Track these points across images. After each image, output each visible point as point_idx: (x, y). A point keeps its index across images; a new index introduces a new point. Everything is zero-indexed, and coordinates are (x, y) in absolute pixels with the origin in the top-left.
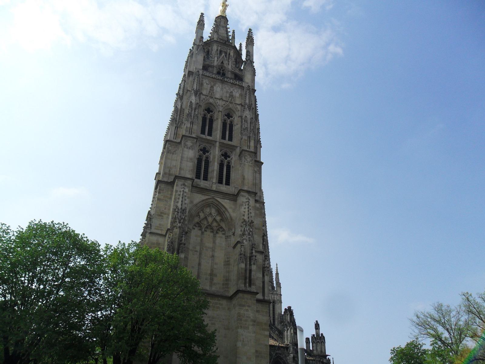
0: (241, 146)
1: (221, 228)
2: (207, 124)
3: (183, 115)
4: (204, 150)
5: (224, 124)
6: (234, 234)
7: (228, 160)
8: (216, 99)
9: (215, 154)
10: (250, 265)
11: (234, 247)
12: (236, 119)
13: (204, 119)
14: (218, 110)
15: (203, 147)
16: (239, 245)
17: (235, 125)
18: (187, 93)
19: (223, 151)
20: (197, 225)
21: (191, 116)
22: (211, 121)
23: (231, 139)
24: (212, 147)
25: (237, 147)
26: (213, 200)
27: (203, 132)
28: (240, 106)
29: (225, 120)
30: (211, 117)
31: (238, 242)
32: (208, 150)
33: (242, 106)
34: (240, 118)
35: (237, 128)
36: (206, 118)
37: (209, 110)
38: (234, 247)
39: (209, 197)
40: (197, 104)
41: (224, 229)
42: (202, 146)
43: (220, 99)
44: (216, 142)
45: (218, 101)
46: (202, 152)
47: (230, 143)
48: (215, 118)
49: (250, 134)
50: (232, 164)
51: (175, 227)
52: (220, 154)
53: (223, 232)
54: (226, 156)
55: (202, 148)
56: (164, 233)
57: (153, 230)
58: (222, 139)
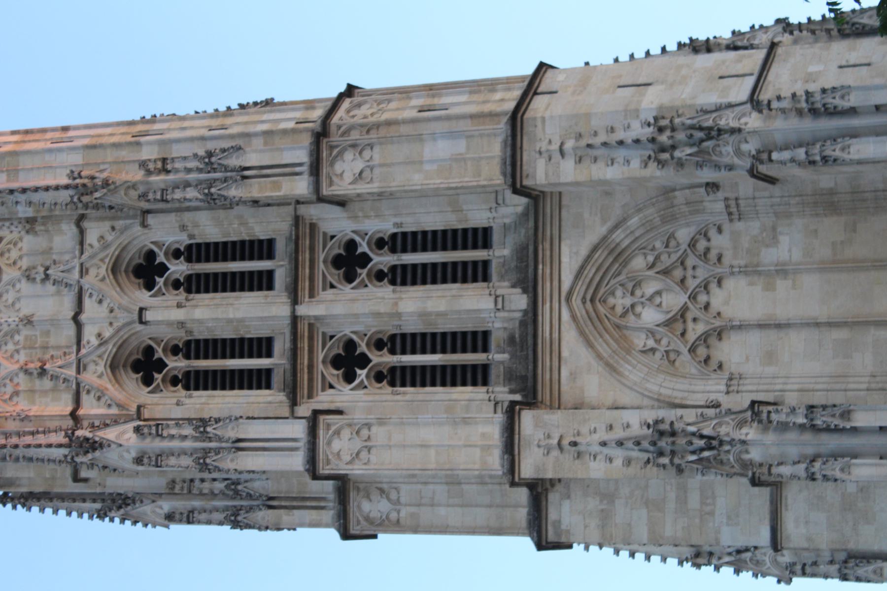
0: (293, 202)
1: (692, 244)
2: (221, 363)
3: (202, 480)
4: (349, 361)
5: (195, 285)
6: (712, 186)
7: (371, 249)
8: (84, 342)
9: (355, 309)
10: (853, 111)
11: (771, 180)
12: (165, 233)
13: (195, 381)
14: (139, 327)
15: (335, 372)
16: (763, 169)
17: (191, 236)
18: (86, 480)
19: (331, 274)
20: (702, 351)
21: (206, 452)
22: (195, 348)
23: (263, 248)
24: (330, 331)
25: (297, 220)
26: (576, 301)
27: (259, 380)
28: (86, 224)
29: (177, 285)
30: (175, 350)
31: (753, 173)
32: (341, 345)
33: (82, 217)
34: (151, 220)
35: (211, 228)
36: (187, 374)
37: (146, 366)
38: (771, 180)
39: (566, 315)
40: (143, 434)
41: (699, 233)
42: (333, 374)
43: (79, 326)
44: (295, 319)
45: (90, 335)
46: (362, 374)
47: (280, 247)
48: (181, 337)
49: (226, 169)
50: (386, 226)
51: (739, 460)
52: (347, 288)
53: (712, 233)
54: (349, 262)
55: (340, 372)
56: (764, 493)
57: (764, 537)
58: (270, 287)
